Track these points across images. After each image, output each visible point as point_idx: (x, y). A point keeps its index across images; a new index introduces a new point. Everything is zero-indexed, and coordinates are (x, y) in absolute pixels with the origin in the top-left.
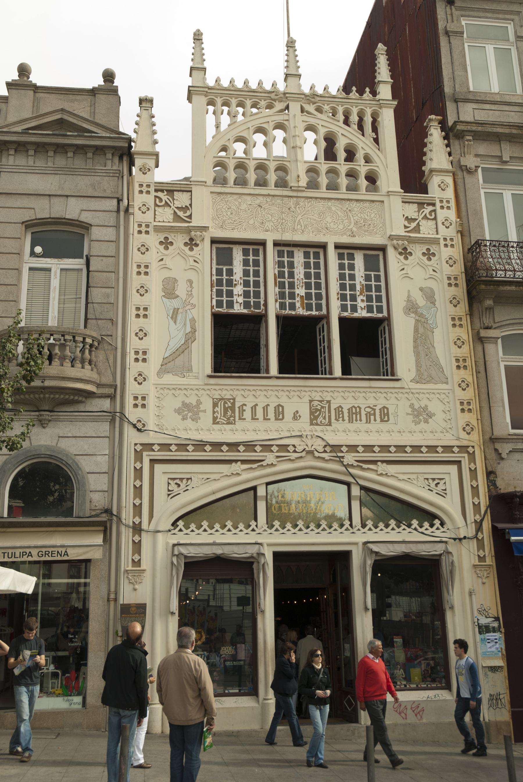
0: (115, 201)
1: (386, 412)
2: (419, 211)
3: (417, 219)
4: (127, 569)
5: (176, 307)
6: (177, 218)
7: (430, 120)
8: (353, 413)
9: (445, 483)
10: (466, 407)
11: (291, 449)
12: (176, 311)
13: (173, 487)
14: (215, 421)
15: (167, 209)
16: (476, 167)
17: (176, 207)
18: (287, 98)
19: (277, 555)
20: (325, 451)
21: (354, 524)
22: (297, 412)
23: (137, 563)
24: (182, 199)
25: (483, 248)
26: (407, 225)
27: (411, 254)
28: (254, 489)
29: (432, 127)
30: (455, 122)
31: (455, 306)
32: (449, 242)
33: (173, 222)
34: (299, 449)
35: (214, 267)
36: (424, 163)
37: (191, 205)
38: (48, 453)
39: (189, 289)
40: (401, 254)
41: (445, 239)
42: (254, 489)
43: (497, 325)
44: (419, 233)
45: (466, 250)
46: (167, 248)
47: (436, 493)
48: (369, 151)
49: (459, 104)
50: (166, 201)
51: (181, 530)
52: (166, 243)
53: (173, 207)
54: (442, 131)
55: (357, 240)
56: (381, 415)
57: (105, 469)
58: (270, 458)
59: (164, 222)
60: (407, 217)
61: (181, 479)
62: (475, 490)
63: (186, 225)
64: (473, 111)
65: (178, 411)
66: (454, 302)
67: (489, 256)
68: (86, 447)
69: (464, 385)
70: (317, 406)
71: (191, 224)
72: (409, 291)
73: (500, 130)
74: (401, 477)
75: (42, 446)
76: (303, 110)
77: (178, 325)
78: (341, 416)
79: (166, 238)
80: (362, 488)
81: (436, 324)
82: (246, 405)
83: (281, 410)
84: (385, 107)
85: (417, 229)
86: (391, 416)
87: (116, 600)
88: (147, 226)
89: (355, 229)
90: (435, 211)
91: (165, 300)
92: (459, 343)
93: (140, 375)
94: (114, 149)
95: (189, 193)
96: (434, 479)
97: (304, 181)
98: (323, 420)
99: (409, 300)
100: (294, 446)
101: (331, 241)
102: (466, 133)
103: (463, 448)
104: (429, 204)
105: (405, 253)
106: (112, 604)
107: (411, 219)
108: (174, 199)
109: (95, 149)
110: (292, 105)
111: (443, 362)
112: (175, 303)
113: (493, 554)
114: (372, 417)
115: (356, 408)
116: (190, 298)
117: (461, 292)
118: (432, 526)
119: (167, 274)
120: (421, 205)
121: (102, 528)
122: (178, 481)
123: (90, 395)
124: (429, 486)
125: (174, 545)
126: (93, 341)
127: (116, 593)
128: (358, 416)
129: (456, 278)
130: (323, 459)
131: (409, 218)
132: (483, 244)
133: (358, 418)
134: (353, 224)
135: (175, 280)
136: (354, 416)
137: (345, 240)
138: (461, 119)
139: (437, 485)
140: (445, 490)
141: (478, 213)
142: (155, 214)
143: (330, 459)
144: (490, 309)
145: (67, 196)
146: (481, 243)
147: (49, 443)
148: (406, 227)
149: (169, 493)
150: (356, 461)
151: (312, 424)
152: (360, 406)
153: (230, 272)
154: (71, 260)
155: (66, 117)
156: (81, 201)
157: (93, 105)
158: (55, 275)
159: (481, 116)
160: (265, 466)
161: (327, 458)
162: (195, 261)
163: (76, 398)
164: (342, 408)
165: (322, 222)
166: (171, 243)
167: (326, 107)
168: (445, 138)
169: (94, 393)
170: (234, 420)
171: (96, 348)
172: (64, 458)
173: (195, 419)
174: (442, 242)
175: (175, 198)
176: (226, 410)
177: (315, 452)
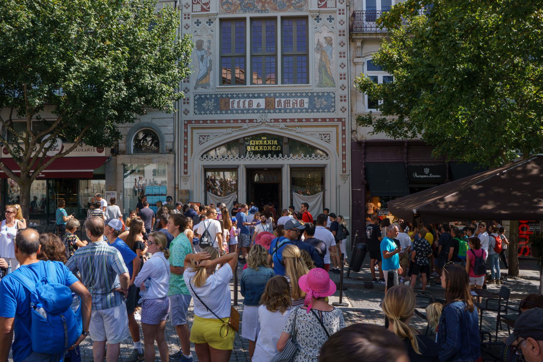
6: (203, 10)
10: (343, 99)
11: (255, 121)
12: (202, 56)
13: (201, 139)
15: (198, 5)
17: (203, 4)
20: (271, 122)
22: (259, 103)
23: (186, 173)
25: (357, 15)
26: (320, 3)
27: (321, 19)
28: (238, 139)
32: (341, 12)
33: (201, 11)
34: (259, 121)
40: (315, 19)
41: (340, 10)
43: (364, 55)
44: (326, 8)
45: (351, 14)
46: (198, 25)
51: (205, 159)
52: (198, 23)
57: (172, 132)
58: (245, 125)
59: (197, 12)
61: (205, 136)
62: (344, 140)
66: (342, 44)
68: (164, 122)
69: (343, 88)
72: (319, 39)
79: (198, 20)
80: (289, 138)
86: (305, 104)
87: (178, 188)
92: (343, 66)
93: (186, 88)
96: (324, 134)
99: (319, 44)
100: (256, 120)
101: (279, 15)
103: (339, 120)
105: (318, 19)
106: (177, 190)
111: (334, 76)
112: (203, 53)
113: (350, 169)
114: (296, 105)
117: (345, 39)
119: (198, 38)
122: (203, 137)
127: (178, 185)
135: (202, 41)
139: (325, 137)
161: (272, 125)
162: (211, 31)
166: (200, 23)
172: (154, 128)
176: (226, 103)
177: (266, 123)
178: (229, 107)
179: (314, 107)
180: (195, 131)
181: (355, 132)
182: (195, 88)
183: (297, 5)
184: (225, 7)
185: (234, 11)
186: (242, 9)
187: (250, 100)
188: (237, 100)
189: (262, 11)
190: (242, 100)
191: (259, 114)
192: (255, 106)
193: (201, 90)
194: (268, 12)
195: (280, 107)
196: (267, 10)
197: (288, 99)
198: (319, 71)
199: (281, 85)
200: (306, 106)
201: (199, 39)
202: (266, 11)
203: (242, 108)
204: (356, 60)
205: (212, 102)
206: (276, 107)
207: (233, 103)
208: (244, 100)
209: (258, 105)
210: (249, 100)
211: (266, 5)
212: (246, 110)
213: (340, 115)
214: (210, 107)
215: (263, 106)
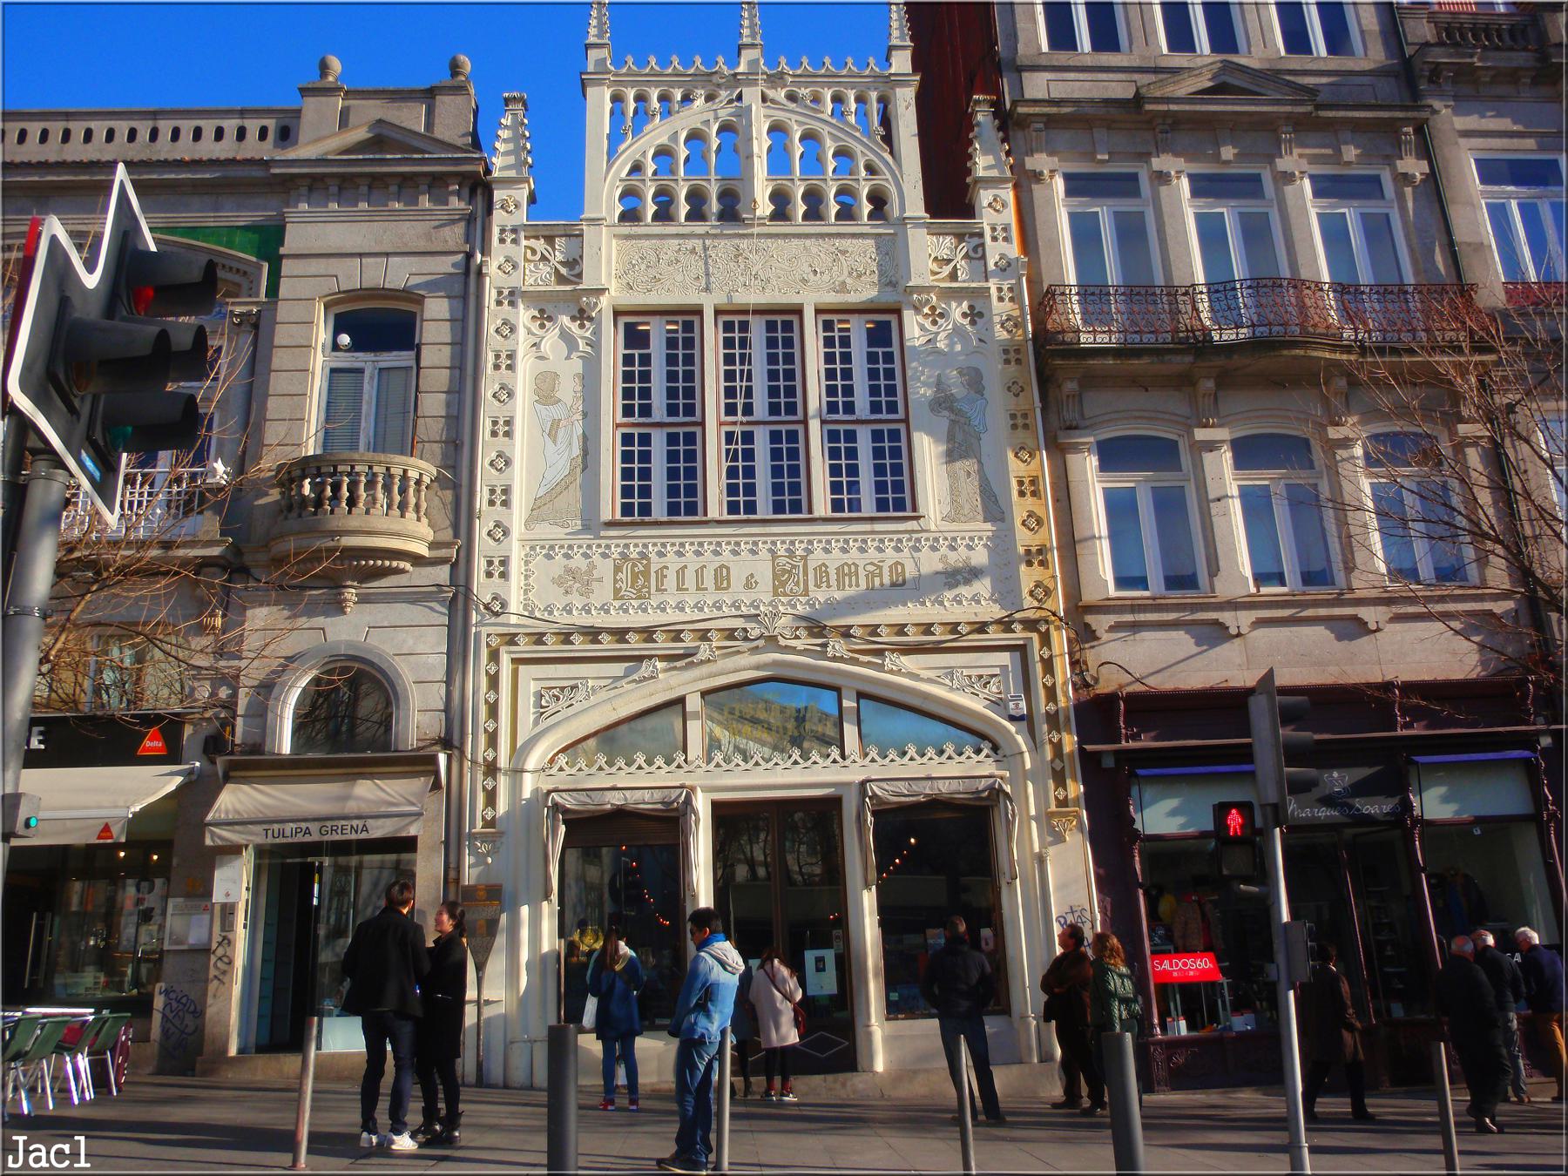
2: (956, 248)
3: (949, 261)
7: (978, 102)
14: (617, 594)
19: (717, 806)
20: (797, 637)
21: (847, 752)
22: (752, 575)
28: (681, 701)
31: (1017, 395)
34: (754, 633)
35: (622, 351)
36: (969, 172)
37: (581, 257)
38: (350, 652)
41: (1000, 290)
42: (681, 701)
43: (1088, 423)
48: (872, 157)
53: (552, 261)
55: (853, 298)
61: (562, 689)
65: (558, 581)
66: (1015, 389)
71: (580, 287)
73: (1088, 110)
74: (925, 674)
75: (339, 642)
76: (764, 99)
80: (861, 695)
81: (985, 425)
82: (667, 568)
83: (725, 573)
85: (953, 276)
89: (849, 281)
90: (983, 245)
91: (538, 406)
94: (462, 177)
96: (981, 677)
97: (765, 208)
100: (745, 630)
102: (1033, 119)
104: (972, 235)
108: (554, 249)
110: (747, 91)
112: (556, 412)
115: (849, 566)
118: (978, 751)
119: (543, 366)
120: (960, 237)
123: (417, 560)
125: (549, 792)
126: (421, 474)
130: (793, 650)
134: (846, 273)
136: (847, 578)
137: (831, 299)
138: (1027, 96)
141: (1055, 244)
145: (387, 255)
147: (353, 638)
151: (776, 594)
152: (857, 562)
153: (646, 360)
154: (395, 353)
155: (386, 132)
156: (407, 259)
157: (430, 113)
158: (372, 378)
159: (1058, 92)
163: (395, 564)
164: (827, 567)
168: (999, 129)
169: (423, 557)
170: (649, 592)
172: (376, 660)
173: (586, 591)
174: (994, 292)
176: (635, 576)
180: (522, 668)
182: (528, 523)
199: (823, 514)
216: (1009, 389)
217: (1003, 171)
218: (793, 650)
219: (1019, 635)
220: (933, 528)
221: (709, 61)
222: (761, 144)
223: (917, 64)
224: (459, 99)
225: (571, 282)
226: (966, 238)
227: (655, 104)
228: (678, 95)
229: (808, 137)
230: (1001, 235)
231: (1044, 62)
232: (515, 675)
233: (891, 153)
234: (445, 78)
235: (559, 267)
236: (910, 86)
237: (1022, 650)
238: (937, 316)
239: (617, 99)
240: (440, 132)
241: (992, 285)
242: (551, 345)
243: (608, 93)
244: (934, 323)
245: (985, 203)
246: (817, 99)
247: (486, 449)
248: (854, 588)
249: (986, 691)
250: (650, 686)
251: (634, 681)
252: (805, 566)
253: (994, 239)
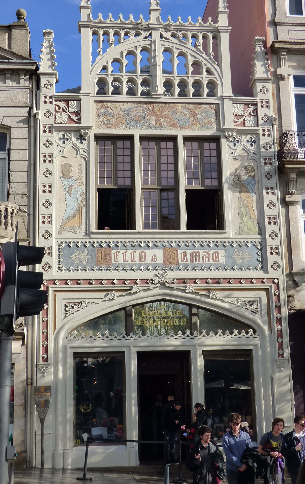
0: (27, 109)
1: (217, 255)
3: (243, 116)
4: (39, 363)
5: (71, 185)
8: (193, 256)
9: (257, 304)
11: (149, 281)
12: (70, 187)
16: (288, 75)
17: (70, 113)
18: (150, 27)
20: (173, 283)
22: (155, 256)
24: (73, 106)
25: (289, 137)
26: (236, 120)
29: (257, 46)
30: (274, 43)
34: (156, 281)
37: (80, 110)
39: (80, 171)
41: (264, 130)
47: (251, 311)
48: (209, 66)
49: (278, 27)
50: (63, 109)
52: (64, 139)
53: (68, 112)
54: (264, 49)
56: (213, 257)
58: (135, 288)
59: (61, 123)
60: (236, 115)
61: (75, 303)
63: (77, 125)
64: (289, 32)
67: (294, 142)
70: (168, 252)
71: (81, 125)
76: (161, 36)
77: (72, 197)
78: (185, 258)
82: (119, 252)
83: (143, 255)
84: (222, 32)
86: (221, 258)
87: (31, 383)
88: (50, 127)
91: (62, 179)
94: (26, 72)
95: (79, 102)
96: (249, 301)
98: (173, 261)
100: (152, 280)
101: (180, 134)
104: (252, 105)
106: (29, 386)
107: (239, 116)
109: (11, 71)
110: (153, 32)
112: (70, 182)
114: (207, 259)
116: (81, 178)
118: (247, 333)
121: (21, 337)
124: (246, 306)
126: (13, 210)
128: (197, 258)
129: (270, 159)
130: (172, 288)
131: (238, 115)
132: (289, 134)
133: (197, 260)
135: (70, 166)
136: (194, 258)
139: (251, 305)
140: (257, 309)
142: (55, 118)
143: (177, 289)
144: (294, 181)
146: (288, 133)
148: (235, 122)
149: (66, 312)
150: (194, 289)
152: (199, 251)
160: (132, 293)
162: (84, 151)
165: (174, 120)
167: (179, 34)
171: (16, 215)
174: (261, 133)
175: (69, 105)
176: (105, 256)
177: (166, 283)
178: (111, 261)
179: (234, 263)
180: (58, 294)
181: (291, 299)
182: (60, 233)
183: (205, 121)
184: (103, 119)
185: (117, 126)
186: (127, 123)
187: (142, 252)
188: (122, 251)
189: (155, 127)
190: (130, 251)
191: (155, 272)
192: (148, 260)
193: (68, 236)
194: (164, 130)
195: (185, 262)
196: (163, 126)
197: (196, 251)
198: (239, 213)
200: (222, 260)
201: (64, 162)
202: (161, 127)
203: (130, 262)
204: (288, 198)
205: (85, 253)
206: (180, 262)
207: (116, 255)
208: (132, 251)
209: (154, 258)
210: (140, 251)
211: (162, 120)
212: (135, 265)
213: (272, 274)
214: (82, 260)
215: (160, 260)
216: (266, 176)
217: (268, 75)
218: (171, 288)
219: (267, 285)
220: (231, 237)
221: (137, 17)
222: (160, 59)
223: (231, 21)
224: (23, 31)
225: (76, 123)
226: (250, 106)
227: (112, 38)
228: (122, 33)
229: (181, 54)
230: (265, 104)
231: (287, 21)
232: (55, 296)
233: (218, 65)
234: (13, 20)
235: (71, 115)
236: (227, 32)
237: (267, 290)
238: (236, 142)
239: (95, 33)
240: (16, 49)
241: (260, 128)
242: (67, 151)
243: (90, 31)
244: (235, 145)
245: (258, 90)
246: (185, 36)
247: (41, 198)
248: (197, 262)
249: (252, 308)
250: (113, 302)
251: (106, 300)
252: (177, 252)
253: (262, 107)
